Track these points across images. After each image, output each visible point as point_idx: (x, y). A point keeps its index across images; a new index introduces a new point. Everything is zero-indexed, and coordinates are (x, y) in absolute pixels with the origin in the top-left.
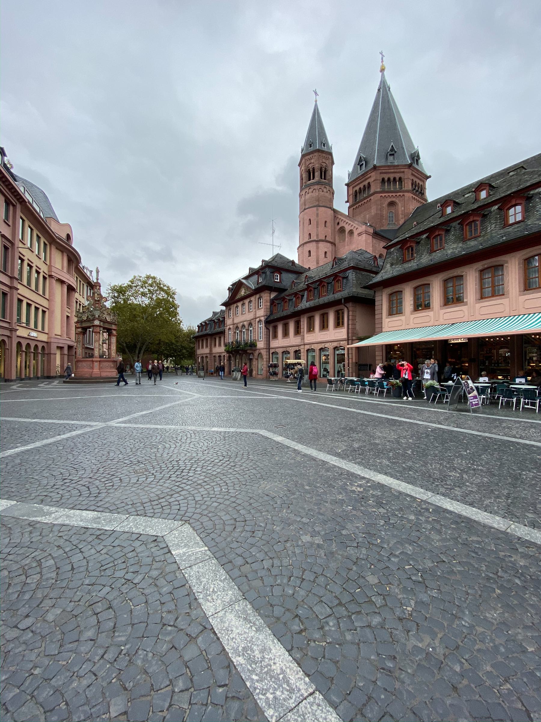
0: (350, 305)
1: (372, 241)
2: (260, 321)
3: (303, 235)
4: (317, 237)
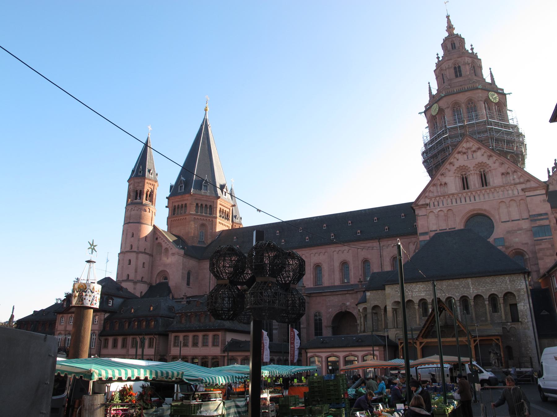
0: (157, 337)
3: (125, 244)
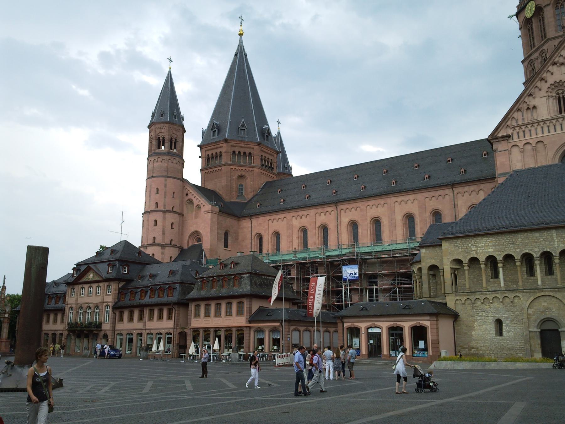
0: (176, 307)
1: (218, 219)
2: (107, 306)
3: (149, 202)
4: (165, 208)
